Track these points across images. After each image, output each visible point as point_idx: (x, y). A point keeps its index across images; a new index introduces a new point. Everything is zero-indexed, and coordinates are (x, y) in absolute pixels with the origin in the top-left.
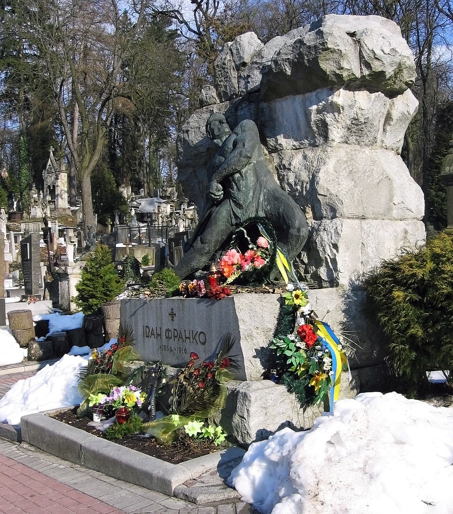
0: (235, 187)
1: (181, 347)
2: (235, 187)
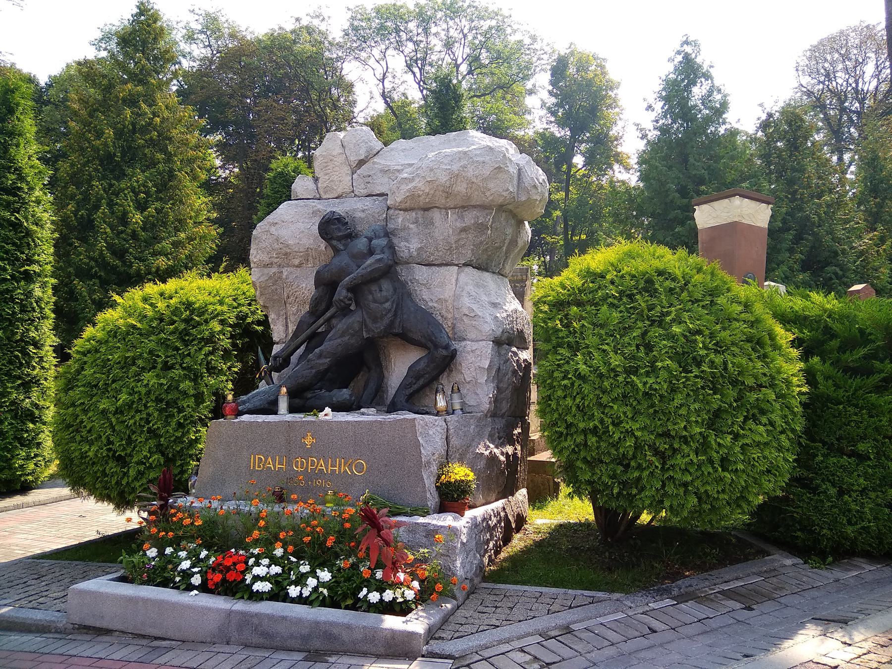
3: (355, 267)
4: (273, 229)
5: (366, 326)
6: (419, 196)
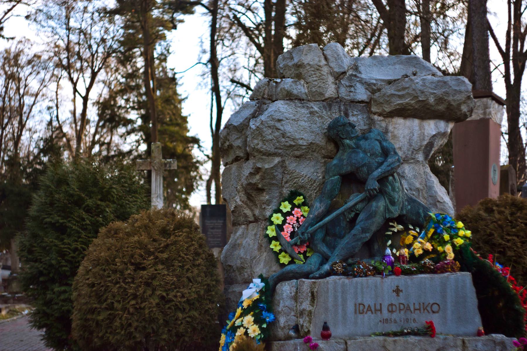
1: (409, 317)
2: (390, 187)
3: (376, 164)
4: (278, 125)
5: (388, 209)
6: (409, 110)
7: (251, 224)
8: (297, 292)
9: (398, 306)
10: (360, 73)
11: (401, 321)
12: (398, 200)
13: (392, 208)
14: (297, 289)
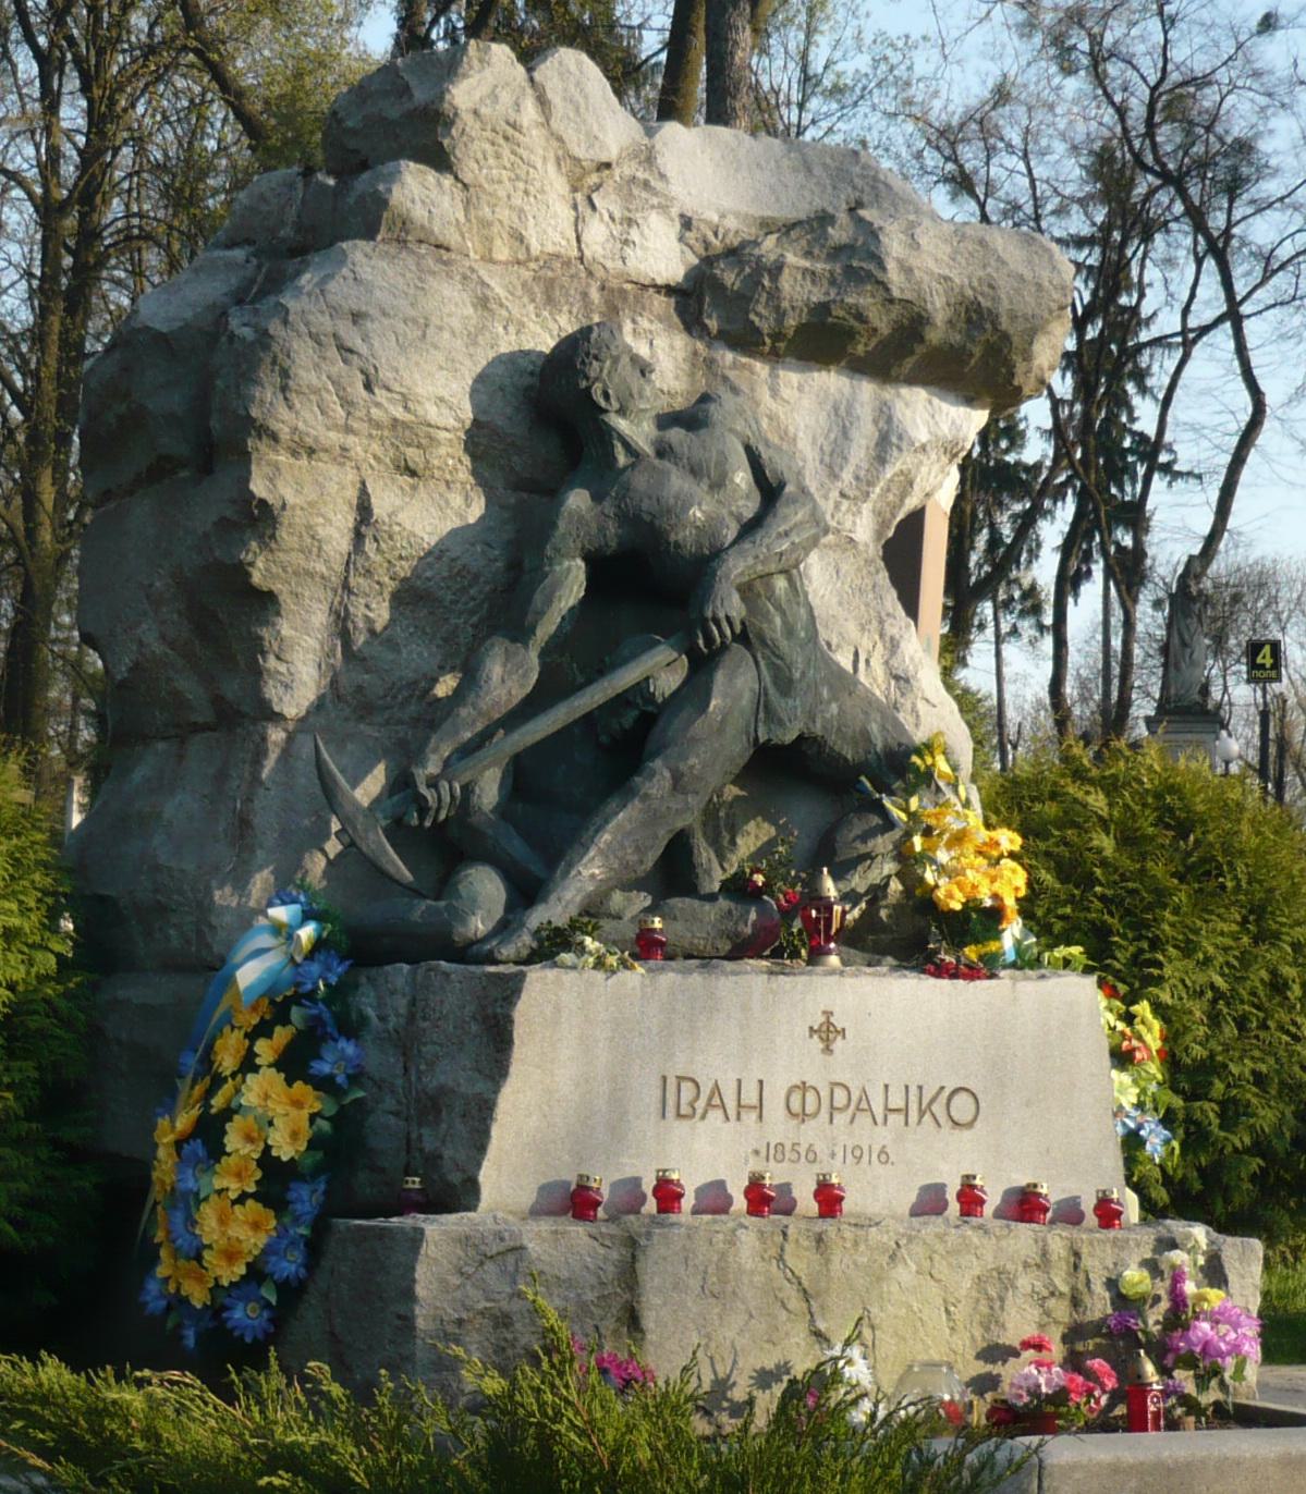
0: (778, 621)
2: (778, 621)
7: (198, 737)
8: (411, 1018)
9: (825, 1094)
10: (662, 176)
11: (833, 1155)
12: (803, 673)
13: (781, 704)
14: (413, 1002)
